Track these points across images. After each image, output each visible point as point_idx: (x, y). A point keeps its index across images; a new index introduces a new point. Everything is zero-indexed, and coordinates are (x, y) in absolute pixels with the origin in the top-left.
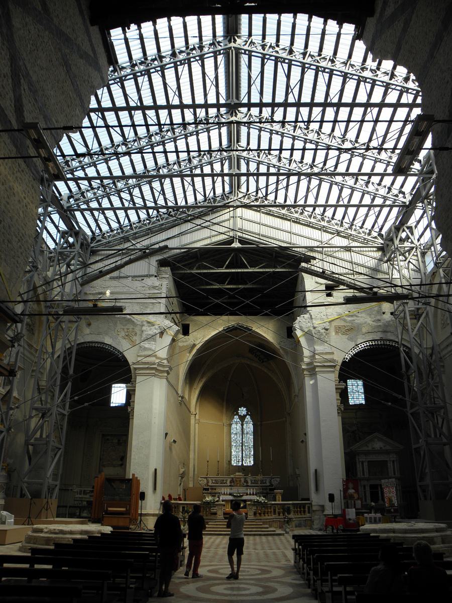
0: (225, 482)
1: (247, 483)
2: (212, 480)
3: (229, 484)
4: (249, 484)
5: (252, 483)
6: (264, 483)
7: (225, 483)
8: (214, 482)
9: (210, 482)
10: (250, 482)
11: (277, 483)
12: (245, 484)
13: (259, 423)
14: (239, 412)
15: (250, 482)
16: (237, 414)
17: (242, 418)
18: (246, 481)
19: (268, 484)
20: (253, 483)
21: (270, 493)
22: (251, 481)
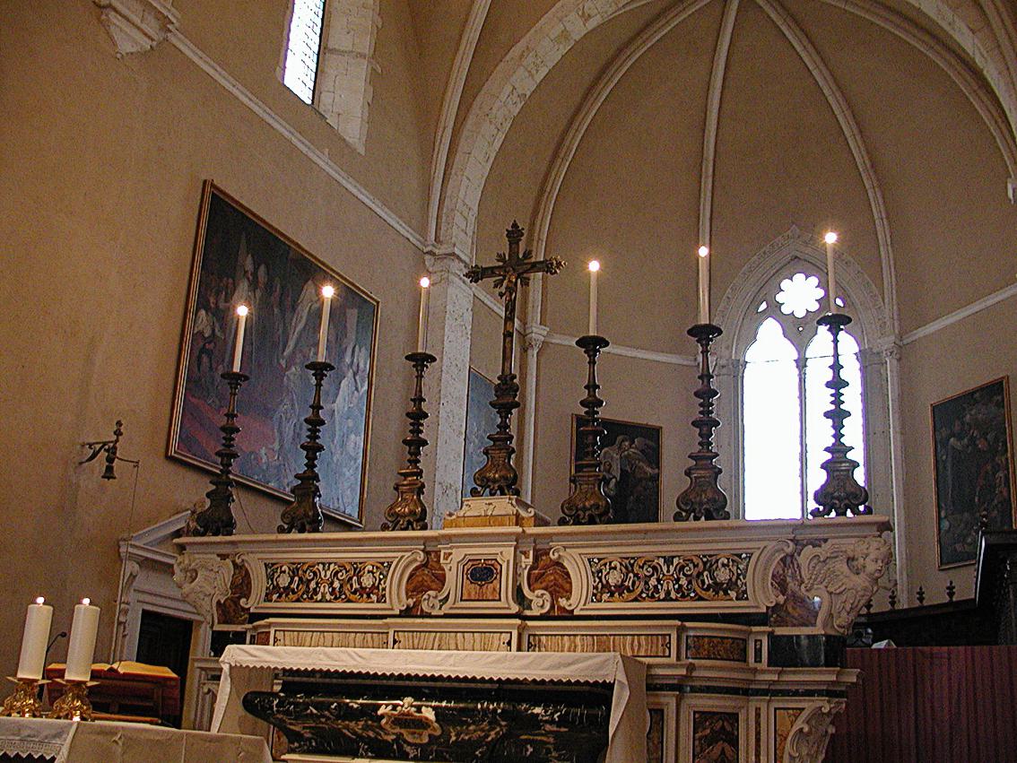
0: (367, 581)
1: (561, 587)
2: (272, 569)
3: (397, 599)
4: (577, 600)
5: (604, 590)
6: (717, 587)
7: (364, 592)
8: (284, 581)
9: (259, 584)
10: (581, 582)
11: (860, 581)
12: (539, 601)
13: (887, 343)
14: (779, 298)
15: (581, 582)
16: (775, 310)
17: (799, 331)
18: (550, 575)
19: (761, 598)
20: (621, 588)
21: (771, 692)
22: (598, 568)
